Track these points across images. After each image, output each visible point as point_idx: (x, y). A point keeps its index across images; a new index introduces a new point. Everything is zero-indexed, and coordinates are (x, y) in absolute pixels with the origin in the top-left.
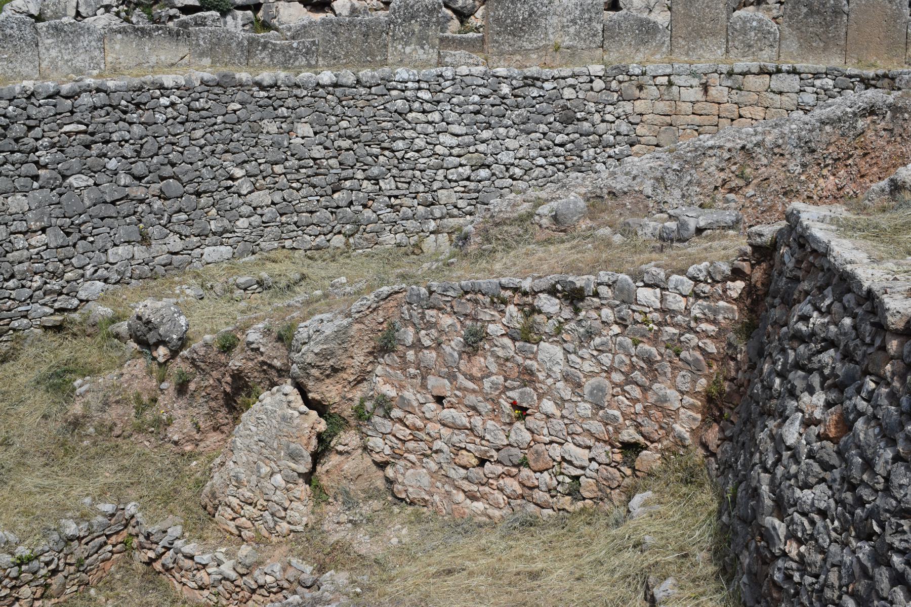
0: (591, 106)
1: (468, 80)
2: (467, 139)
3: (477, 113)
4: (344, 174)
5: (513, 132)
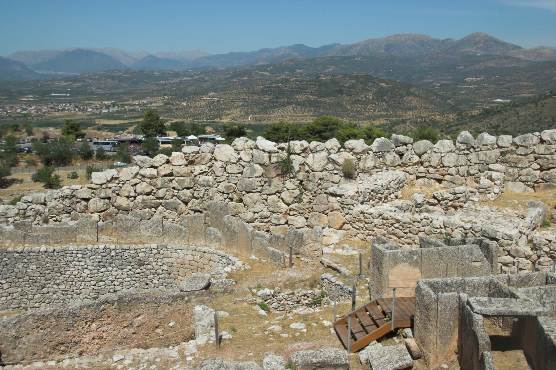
0: (151, 259)
1: (97, 250)
2: (94, 271)
3: (99, 262)
4: (46, 282)
5: (115, 269)
